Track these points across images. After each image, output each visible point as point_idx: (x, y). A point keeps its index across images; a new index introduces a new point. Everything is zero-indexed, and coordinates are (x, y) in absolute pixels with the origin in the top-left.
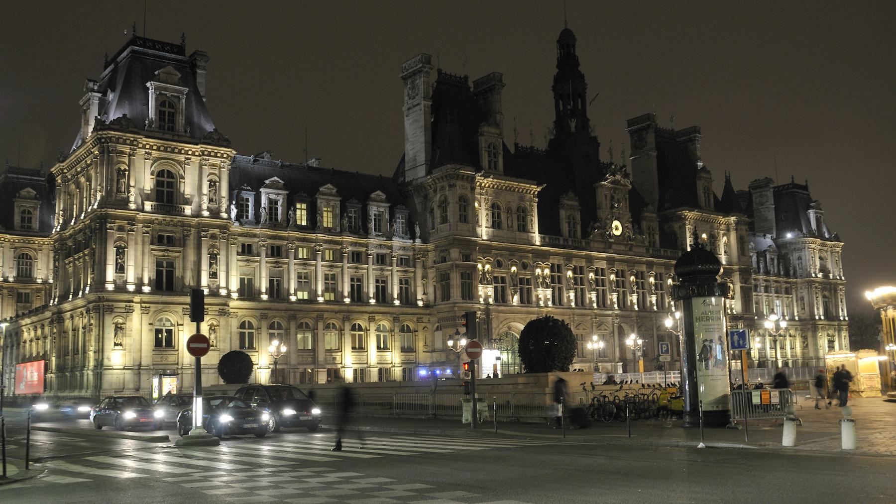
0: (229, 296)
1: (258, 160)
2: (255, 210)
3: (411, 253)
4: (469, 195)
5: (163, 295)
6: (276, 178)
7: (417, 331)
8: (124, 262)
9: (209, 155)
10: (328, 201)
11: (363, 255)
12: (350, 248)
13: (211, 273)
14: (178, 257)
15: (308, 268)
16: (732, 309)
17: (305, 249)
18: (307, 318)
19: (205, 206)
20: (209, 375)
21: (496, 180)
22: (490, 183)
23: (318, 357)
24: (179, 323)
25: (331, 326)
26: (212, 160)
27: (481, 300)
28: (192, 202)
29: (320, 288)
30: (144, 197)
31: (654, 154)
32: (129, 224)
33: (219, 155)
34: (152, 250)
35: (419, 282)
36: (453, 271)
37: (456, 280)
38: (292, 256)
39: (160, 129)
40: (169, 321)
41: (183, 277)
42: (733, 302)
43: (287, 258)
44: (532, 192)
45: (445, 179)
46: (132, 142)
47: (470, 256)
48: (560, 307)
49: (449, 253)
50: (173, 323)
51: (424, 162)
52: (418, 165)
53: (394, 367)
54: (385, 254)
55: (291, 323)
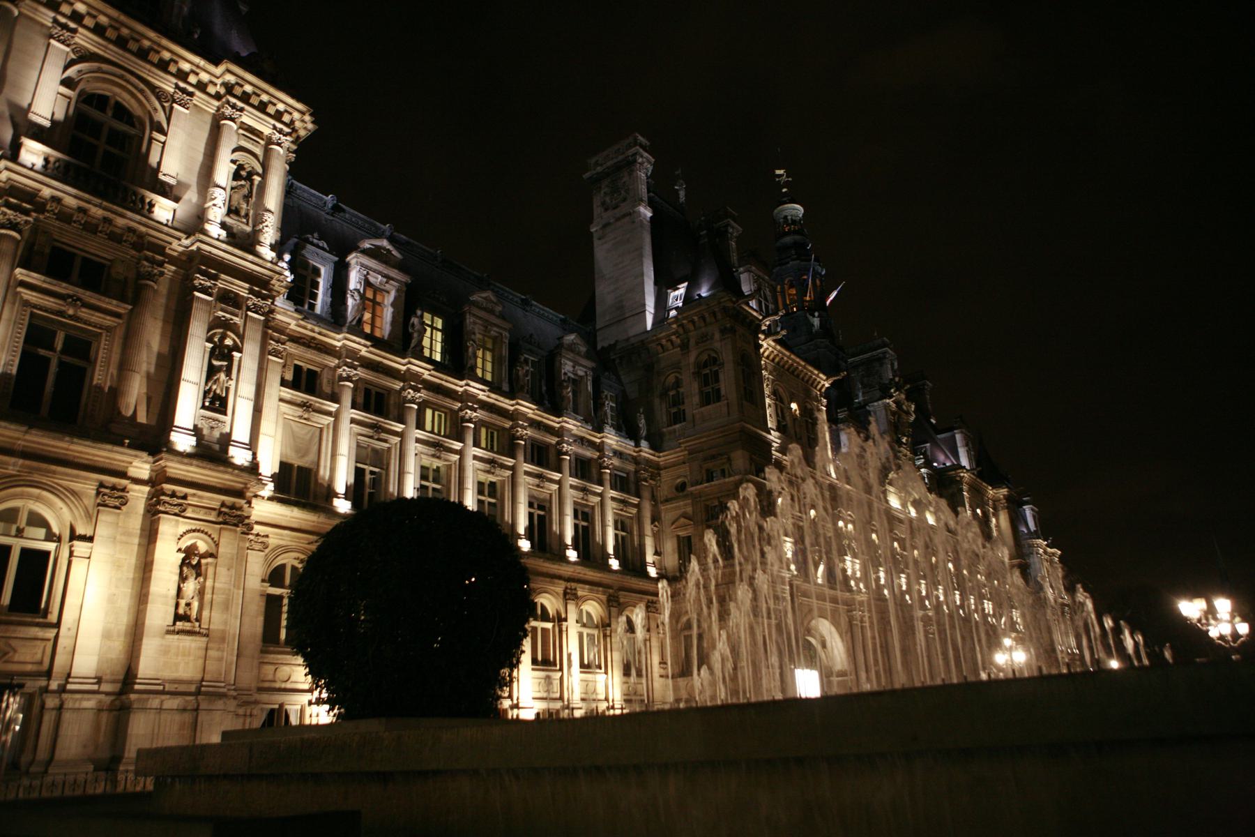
1: (344, 211)
2: (332, 296)
3: (631, 468)
5: (31, 427)
6: (385, 243)
9: (245, 98)
10: (487, 325)
12: (529, 432)
14: (109, 329)
15: (444, 455)
19: (217, 213)
20: (164, 716)
21: (778, 347)
24: (80, 530)
26: (250, 118)
33: (271, 110)
34: (23, 284)
35: (648, 528)
38: (412, 419)
40: (43, 523)
41: (115, 394)
43: (401, 420)
44: (819, 387)
49: (729, 459)
50: (56, 530)
52: (627, 315)
53: (613, 708)
54: (590, 460)
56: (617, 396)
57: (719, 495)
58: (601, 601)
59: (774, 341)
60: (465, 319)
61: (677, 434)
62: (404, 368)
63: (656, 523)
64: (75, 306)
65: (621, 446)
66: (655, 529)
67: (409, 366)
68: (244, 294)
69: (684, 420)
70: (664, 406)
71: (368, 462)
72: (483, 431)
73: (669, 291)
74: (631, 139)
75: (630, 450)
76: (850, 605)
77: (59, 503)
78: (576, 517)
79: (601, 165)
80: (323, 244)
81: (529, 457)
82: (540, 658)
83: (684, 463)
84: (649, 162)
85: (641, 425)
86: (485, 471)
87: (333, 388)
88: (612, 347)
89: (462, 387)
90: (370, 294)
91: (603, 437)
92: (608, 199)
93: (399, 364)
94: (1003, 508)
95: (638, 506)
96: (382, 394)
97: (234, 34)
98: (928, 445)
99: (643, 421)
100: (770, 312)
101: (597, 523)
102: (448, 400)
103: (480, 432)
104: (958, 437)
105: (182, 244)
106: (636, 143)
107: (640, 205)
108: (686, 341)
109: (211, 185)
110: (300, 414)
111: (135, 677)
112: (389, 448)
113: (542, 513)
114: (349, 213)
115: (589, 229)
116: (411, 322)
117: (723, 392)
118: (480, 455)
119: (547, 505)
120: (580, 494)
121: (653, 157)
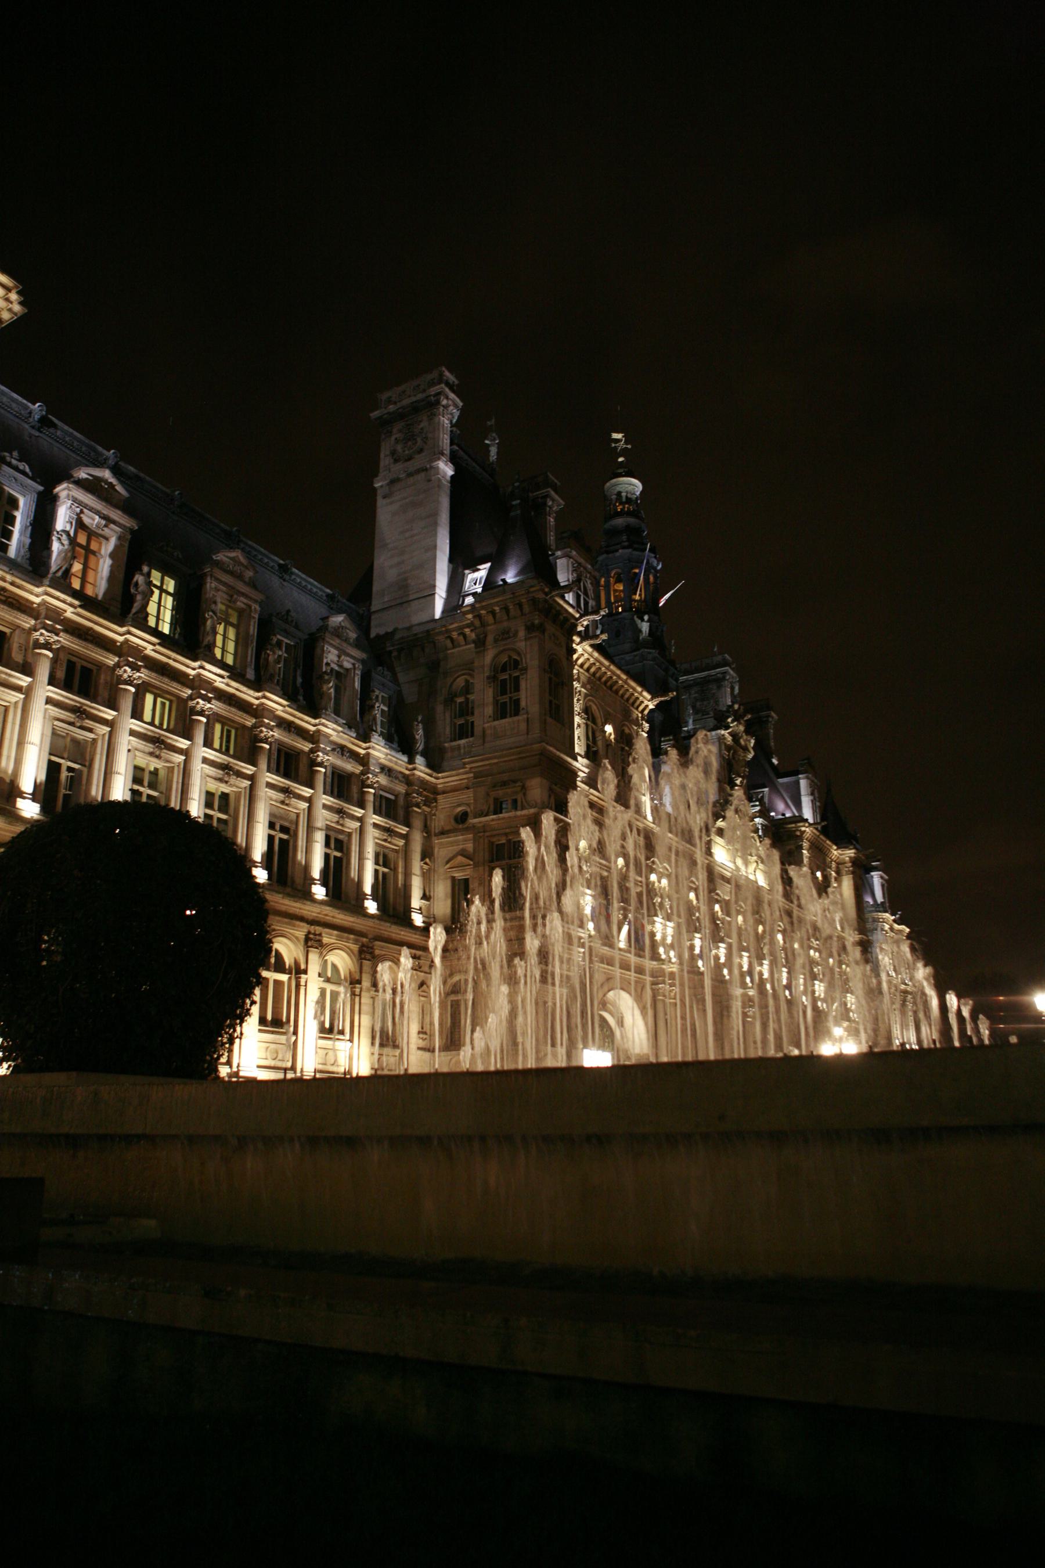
1: (55, 426)
2: (32, 536)
3: (401, 788)
6: (107, 474)
10: (232, 593)
12: (277, 734)
15: (165, 754)
21: (596, 654)
22: (586, 656)
35: (417, 865)
38: (127, 705)
43: (113, 705)
44: (641, 708)
49: (523, 787)
52: (411, 597)
54: (351, 775)
56: (390, 698)
58: (351, 950)
59: (592, 646)
60: (206, 584)
61: (462, 751)
62: (121, 639)
63: (427, 860)
65: (390, 761)
66: (426, 867)
67: (128, 636)
69: (472, 736)
71: (66, 756)
72: (218, 727)
73: (467, 572)
74: (435, 374)
75: (401, 766)
76: (658, 976)
78: (327, 844)
79: (395, 403)
80: (24, 466)
81: (274, 765)
82: (269, 1017)
83: (468, 788)
84: (456, 406)
85: (417, 737)
86: (216, 779)
87: (25, 656)
88: (389, 636)
89: (194, 669)
90: (82, 539)
91: (369, 748)
92: (399, 448)
93: (115, 633)
94: (848, 873)
95: (405, 837)
96: (90, 671)
98: (766, 790)
99: (421, 732)
100: (590, 610)
101: (353, 854)
102: (175, 684)
103: (213, 729)
104: (803, 784)
106: (441, 380)
107: (439, 459)
108: (482, 636)
112: (94, 739)
113: (285, 837)
114: (62, 430)
115: (372, 483)
116: (135, 580)
117: (523, 704)
118: (212, 758)
119: (293, 827)
120: (335, 817)
121: (462, 400)
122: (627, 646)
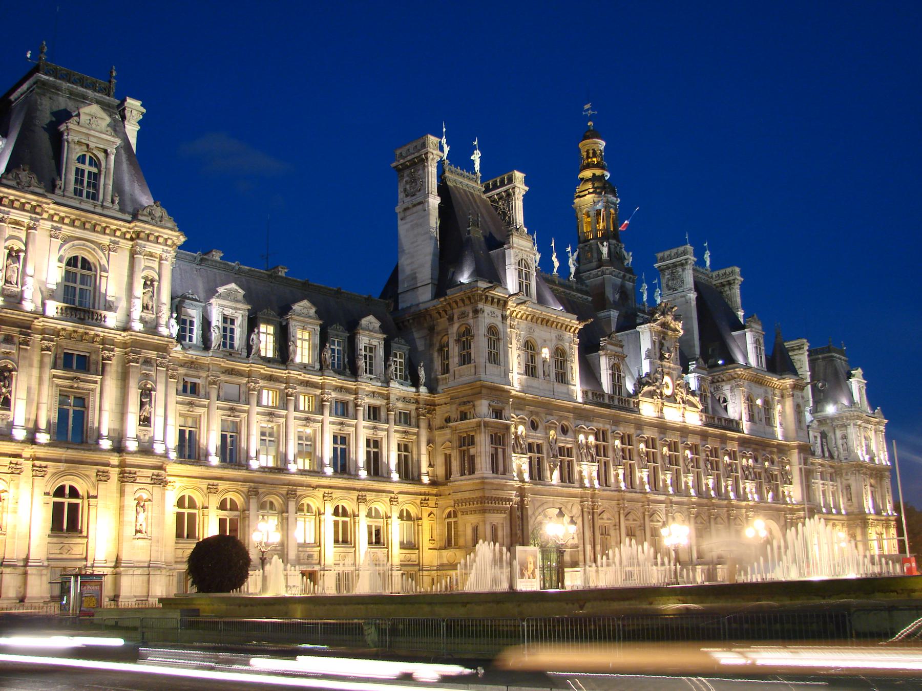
0: (166, 455)
4: (500, 326)
5: (68, 448)
6: (233, 286)
7: (421, 519)
8: (10, 392)
11: (351, 405)
12: (334, 395)
13: (142, 417)
15: (275, 419)
16: (790, 497)
17: (270, 392)
18: (272, 494)
19: (137, 313)
20: (135, 577)
22: (523, 312)
23: (287, 554)
24: (91, 494)
25: (306, 508)
26: (151, 248)
27: (515, 474)
28: (117, 308)
29: (292, 450)
30: (45, 294)
31: (693, 296)
32: (21, 333)
34: (54, 376)
36: (480, 433)
37: (483, 447)
39: (76, 194)
42: (791, 488)
44: (572, 330)
45: (467, 302)
46: (34, 207)
47: (502, 411)
48: (607, 488)
49: (474, 406)
51: (430, 281)
52: (419, 285)
55: (251, 501)
57: (467, 430)
63: (431, 445)
64: (77, 382)
68: (154, 357)
70: (440, 358)
77: (82, 482)
82: (340, 540)
92: (408, 187)
97: (136, 185)
105: (122, 337)
109: (133, 297)
110: (188, 409)
111: (121, 560)
122: (594, 264)
